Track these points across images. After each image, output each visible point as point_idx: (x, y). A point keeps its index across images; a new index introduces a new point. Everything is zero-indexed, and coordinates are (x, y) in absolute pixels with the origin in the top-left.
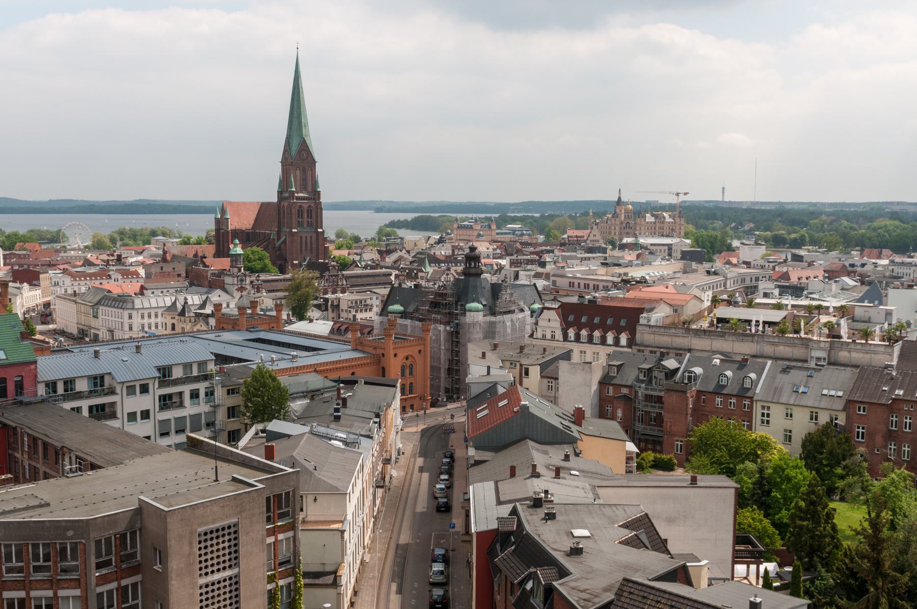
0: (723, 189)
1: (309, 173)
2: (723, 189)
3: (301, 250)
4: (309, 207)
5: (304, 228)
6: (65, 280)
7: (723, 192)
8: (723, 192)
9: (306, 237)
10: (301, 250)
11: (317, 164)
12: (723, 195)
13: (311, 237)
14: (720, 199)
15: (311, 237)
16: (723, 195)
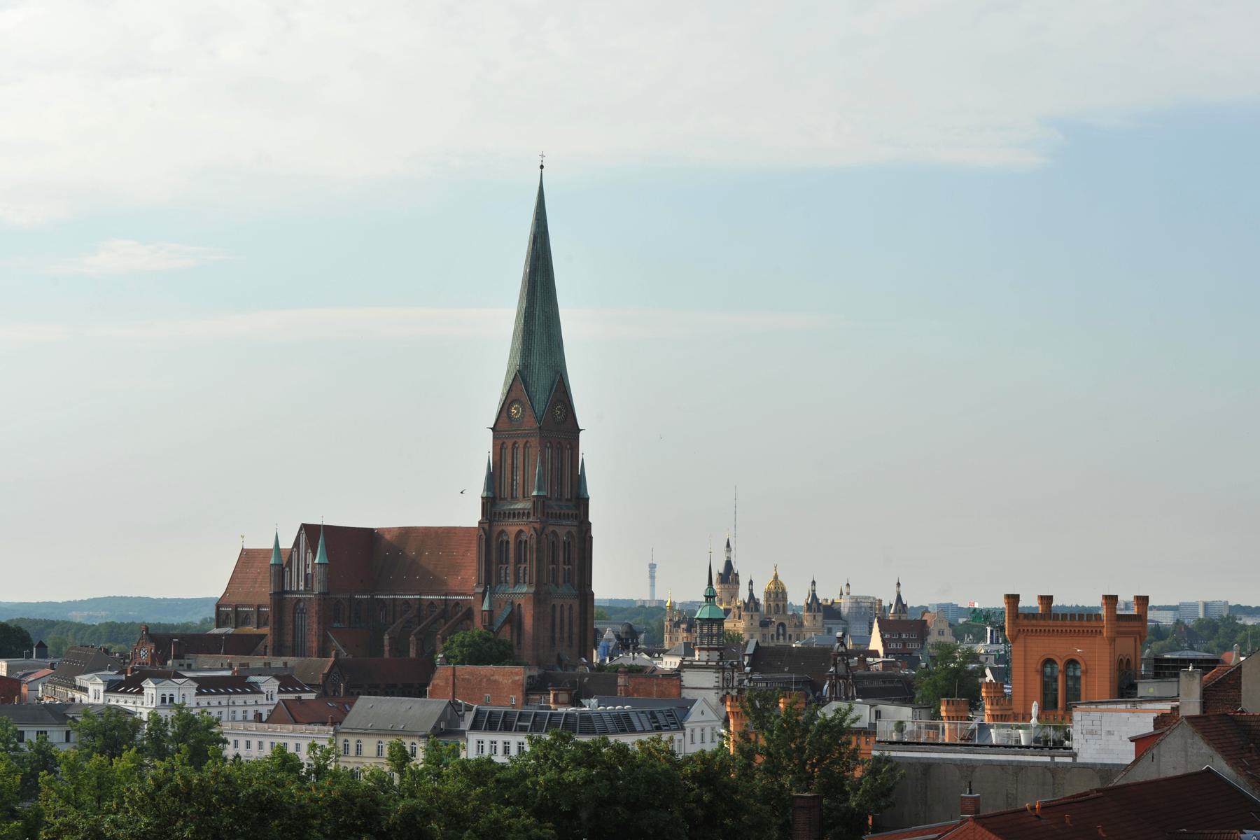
0: (653, 567)
1: (567, 454)
2: (653, 567)
3: (553, 639)
4: (569, 532)
5: (557, 585)
6: (187, 693)
7: (652, 577)
8: (652, 577)
9: (562, 606)
10: (553, 639)
11: (581, 434)
12: (653, 585)
13: (571, 606)
14: (646, 597)
15: (571, 606)
16: (653, 585)
